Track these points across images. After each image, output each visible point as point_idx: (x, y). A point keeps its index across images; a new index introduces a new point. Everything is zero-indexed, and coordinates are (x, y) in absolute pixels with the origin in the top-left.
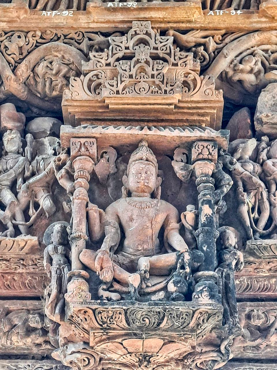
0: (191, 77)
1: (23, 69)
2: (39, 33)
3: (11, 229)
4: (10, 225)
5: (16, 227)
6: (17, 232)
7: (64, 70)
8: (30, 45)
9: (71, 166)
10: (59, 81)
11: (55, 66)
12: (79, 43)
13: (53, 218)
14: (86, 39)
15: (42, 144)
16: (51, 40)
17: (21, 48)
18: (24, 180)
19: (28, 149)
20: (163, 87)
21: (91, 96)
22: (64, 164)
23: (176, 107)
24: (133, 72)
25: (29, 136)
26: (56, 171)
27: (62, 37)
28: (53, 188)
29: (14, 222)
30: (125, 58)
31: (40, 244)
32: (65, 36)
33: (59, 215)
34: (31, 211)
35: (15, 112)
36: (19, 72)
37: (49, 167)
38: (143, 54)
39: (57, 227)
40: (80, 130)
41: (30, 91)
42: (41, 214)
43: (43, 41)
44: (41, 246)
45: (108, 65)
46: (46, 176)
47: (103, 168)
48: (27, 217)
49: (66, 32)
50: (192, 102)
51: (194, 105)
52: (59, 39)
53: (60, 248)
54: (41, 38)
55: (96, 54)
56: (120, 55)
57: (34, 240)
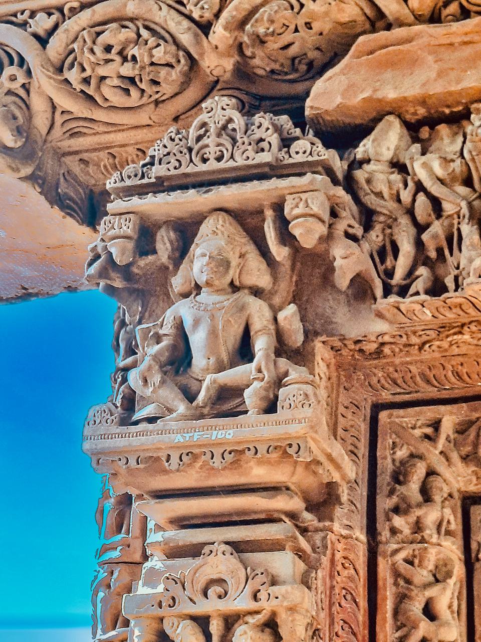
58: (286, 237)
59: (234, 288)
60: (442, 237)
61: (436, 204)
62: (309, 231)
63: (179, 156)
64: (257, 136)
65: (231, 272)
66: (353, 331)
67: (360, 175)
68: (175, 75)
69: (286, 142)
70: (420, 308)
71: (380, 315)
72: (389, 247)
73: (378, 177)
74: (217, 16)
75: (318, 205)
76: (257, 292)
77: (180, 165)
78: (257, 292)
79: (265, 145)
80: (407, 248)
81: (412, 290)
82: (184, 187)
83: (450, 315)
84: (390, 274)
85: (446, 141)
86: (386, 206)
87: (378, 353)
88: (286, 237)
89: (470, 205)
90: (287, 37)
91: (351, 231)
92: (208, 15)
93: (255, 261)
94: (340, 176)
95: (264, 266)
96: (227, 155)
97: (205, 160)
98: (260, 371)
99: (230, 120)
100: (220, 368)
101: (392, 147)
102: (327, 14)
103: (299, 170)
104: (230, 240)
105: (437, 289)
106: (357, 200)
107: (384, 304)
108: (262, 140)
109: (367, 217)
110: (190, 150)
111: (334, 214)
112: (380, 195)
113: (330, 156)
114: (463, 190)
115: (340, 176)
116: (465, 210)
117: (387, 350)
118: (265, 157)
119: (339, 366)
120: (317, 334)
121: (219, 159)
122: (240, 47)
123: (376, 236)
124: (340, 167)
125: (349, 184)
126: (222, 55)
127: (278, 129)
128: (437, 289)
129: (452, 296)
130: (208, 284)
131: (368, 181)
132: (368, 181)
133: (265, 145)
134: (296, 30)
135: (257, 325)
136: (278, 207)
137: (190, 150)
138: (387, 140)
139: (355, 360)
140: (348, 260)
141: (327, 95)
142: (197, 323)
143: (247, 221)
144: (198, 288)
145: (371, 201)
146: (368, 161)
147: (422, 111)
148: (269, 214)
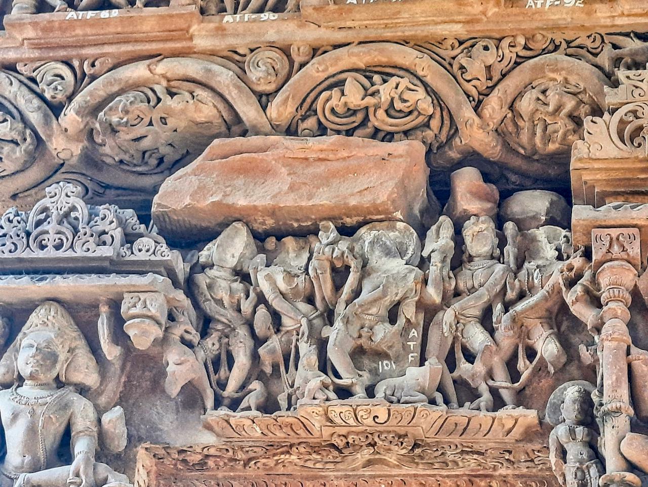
1: (494, 106)
2: (521, 41)
3: (486, 396)
4: (483, 388)
5: (494, 392)
6: (498, 403)
7: (570, 104)
8: (505, 62)
9: (594, 279)
10: (561, 125)
11: (553, 99)
12: (596, 55)
13: (562, 375)
14: (608, 48)
15: (534, 240)
16: (544, 51)
17: (489, 68)
18: (507, 307)
19: (510, 251)
21: (626, 150)
22: (579, 276)
25: (510, 227)
26: (564, 289)
27: (564, 45)
28: (560, 318)
29: (491, 383)
31: (541, 423)
32: (568, 43)
33: (573, 369)
34: (522, 363)
35: (481, 182)
36: (487, 112)
37: (551, 282)
39: (571, 392)
40: (608, 212)
41: (507, 146)
42: (541, 368)
43: (529, 53)
44: (543, 429)
46: (545, 299)
48: (514, 375)
49: (570, 35)
52: (557, 48)
53: (580, 431)
54: (526, 48)
55: (631, 73)
57: (530, 416)
58: (119, 336)
59: (59, 383)
60: (279, 352)
61: (276, 318)
62: (144, 333)
63: (15, 239)
64: (100, 228)
65: (58, 366)
66: (179, 440)
67: (202, 280)
68: (19, 153)
69: (130, 238)
70: (249, 423)
71: (209, 427)
72: (224, 357)
73: (220, 286)
74: (70, 98)
75: (156, 306)
76: (82, 390)
77: (16, 249)
78: (82, 390)
79: (107, 238)
80: (242, 360)
81: (244, 404)
82: (18, 273)
83: (280, 434)
84: (223, 385)
85: (292, 255)
86: (225, 315)
87: (202, 465)
88: (119, 336)
89: (310, 322)
90: (140, 130)
92: (60, 97)
93: (84, 358)
94: (181, 277)
95: (92, 363)
96: (66, 245)
97: (42, 247)
98: (77, 475)
99: (74, 209)
100: (35, 468)
101: (237, 255)
102: (183, 111)
103: (140, 269)
104: (60, 334)
105: (269, 406)
106: (196, 305)
107: (215, 416)
108: (104, 233)
109: (205, 324)
110: (28, 234)
111: (171, 318)
112: (220, 302)
113: (173, 257)
114: (304, 307)
115: (181, 277)
116: (305, 328)
117: (211, 463)
118: (107, 251)
119: (159, 475)
120: (141, 440)
121: (58, 247)
122: (91, 133)
123: (212, 344)
124: (182, 268)
125: (190, 287)
126: (69, 139)
127: (122, 223)
128: (269, 406)
129: (284, 416)
130: (32, 377)
131: (210, 287)
132: (210, 287)
133: (107, 238)
134: (151, 124)
135: (80, 424)
136: (115, 304)
137: (28, 234)
138: (233, 247)
140: (181, 367)
141: (177, 194)
142: (15, 417)
143: (80, 314)
144: (21, 380)
145: (210, 307)
146: (212, 266)
147: (270, 222)
148: (104, 310)
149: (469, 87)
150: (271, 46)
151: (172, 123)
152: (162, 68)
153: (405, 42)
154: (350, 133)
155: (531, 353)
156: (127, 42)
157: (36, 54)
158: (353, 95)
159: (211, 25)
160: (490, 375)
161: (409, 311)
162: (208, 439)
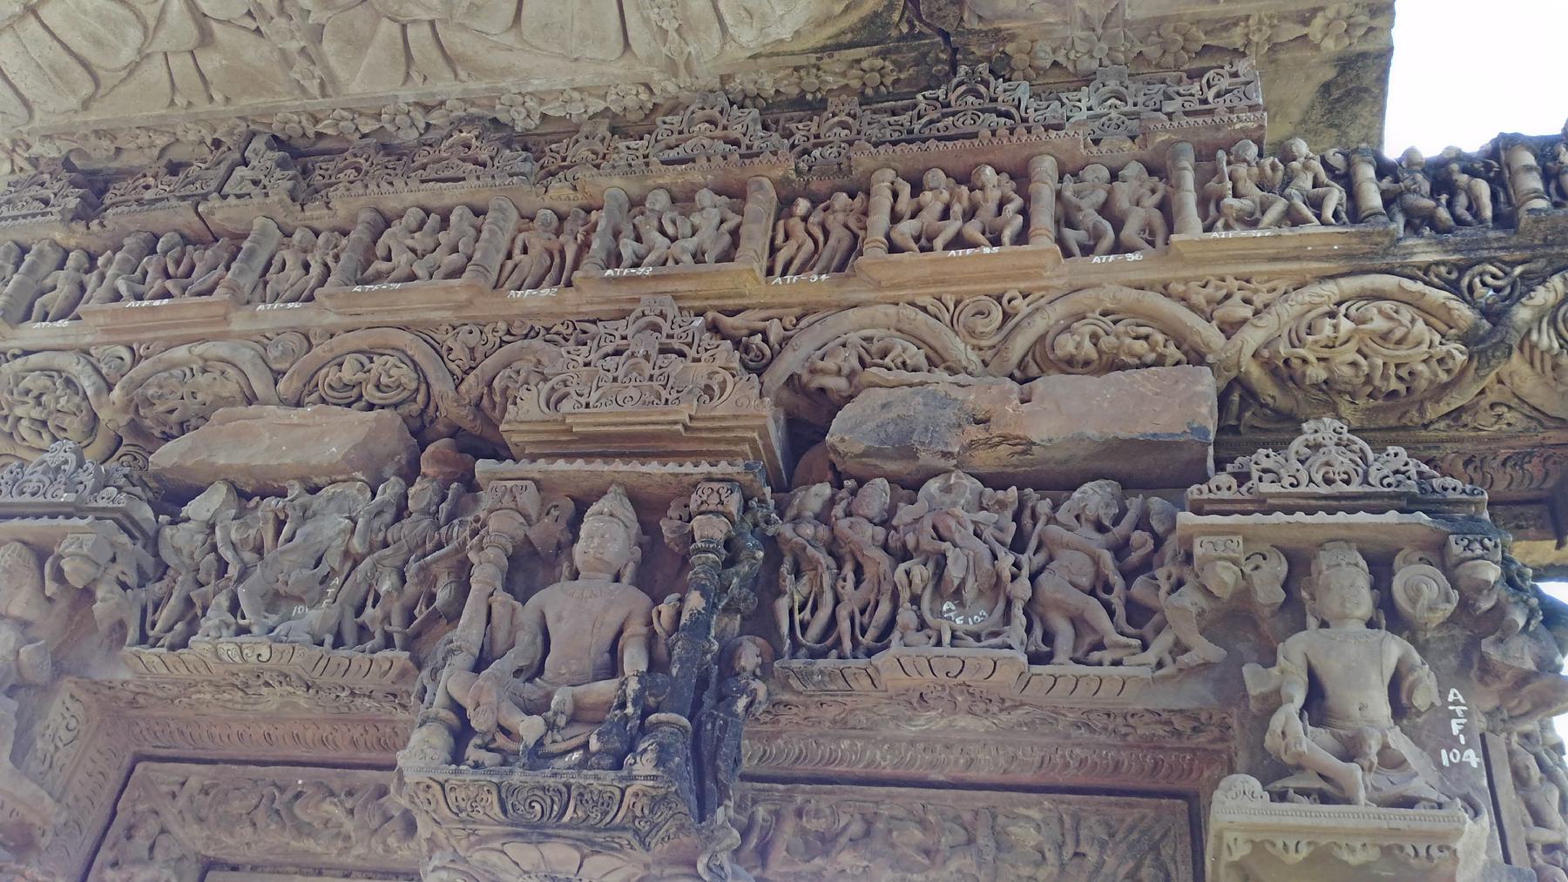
0: (719, 378)
3: (378, 638)
20: (664, 394)
21: (550, 414)
23: (686, 428)
24: (621, 373)
29: (387, 627)
30: (618, 353)
38: (645, 343)
45: (587, 364)
47: (546, 530)
50: (713, 418)
51: (717, 424)
56: (610, 348)
91: (122, 578)
121: (33, 494)
139: (118, 708)
149: (453, 366)
150: (294, 330)
151: (200, 397)
152: (199, 349)
153: (404, 328)
154: (349, 405)
155: (432, 598)
156: (176, 326)
157: (106, 338)
158: (348, 373)
159: (246, 311)
160: (387, 618)
161: (333, 560)
162: (124, 674)
